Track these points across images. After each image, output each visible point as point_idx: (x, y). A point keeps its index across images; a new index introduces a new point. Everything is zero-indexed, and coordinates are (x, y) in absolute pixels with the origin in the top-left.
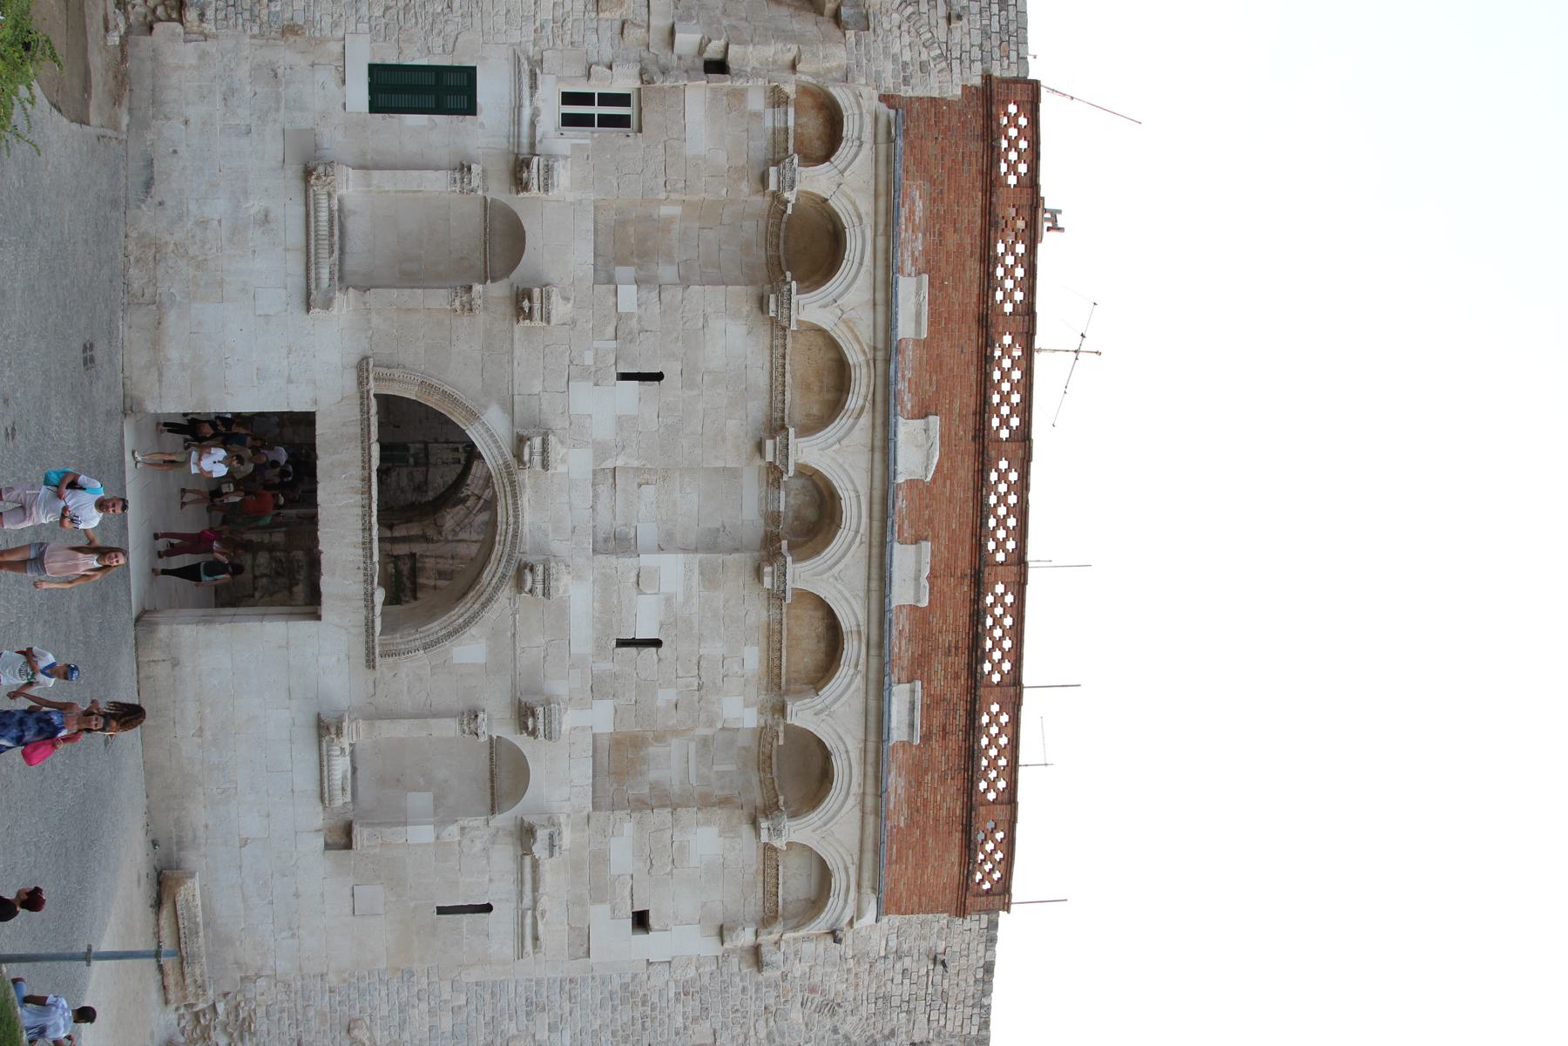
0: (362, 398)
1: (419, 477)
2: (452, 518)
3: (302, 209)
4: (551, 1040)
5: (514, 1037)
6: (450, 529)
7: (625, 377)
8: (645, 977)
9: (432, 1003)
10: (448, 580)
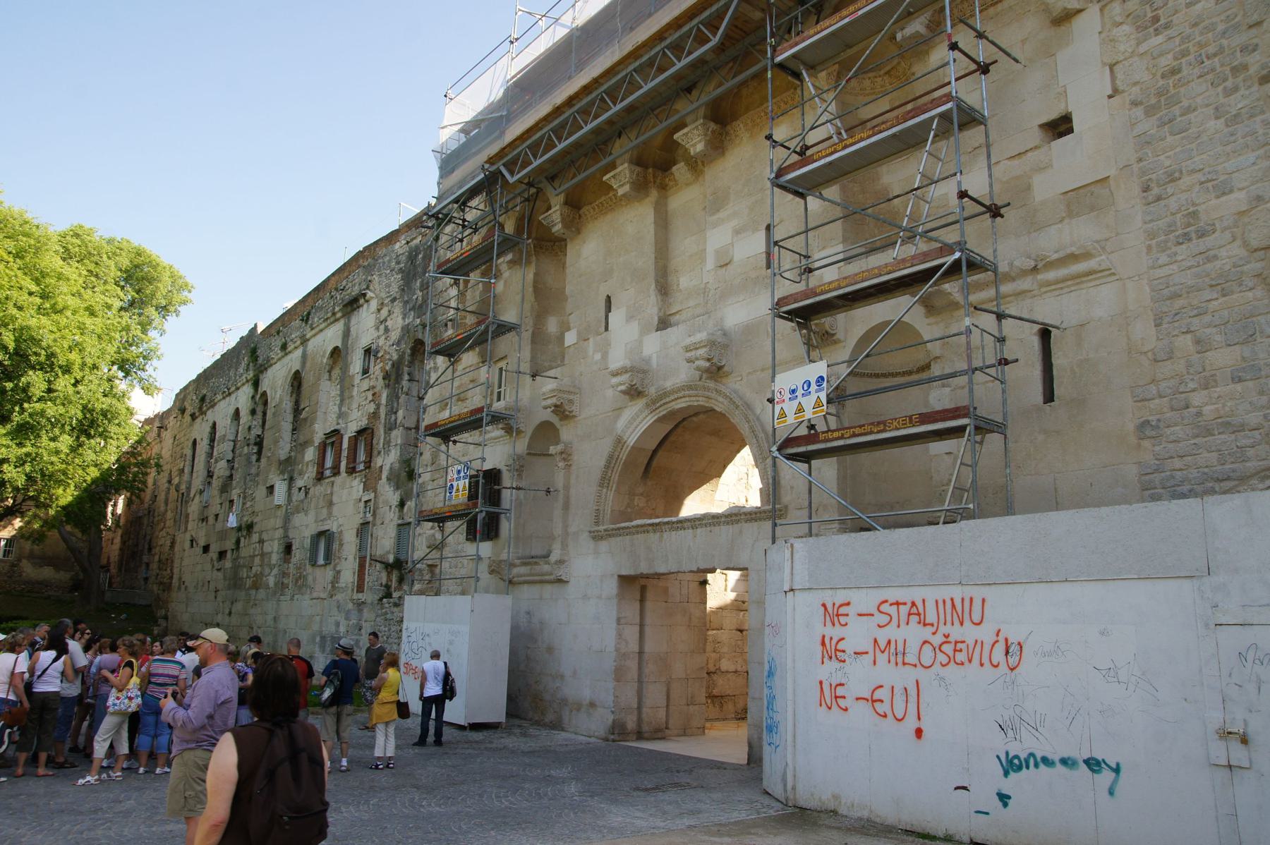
0: (610, 536)
3: (525, 587)
4: (1246, 184)
5: (1245, 244)
7: (607, 329)
8: (1136, 89)
9: (1191, 385)
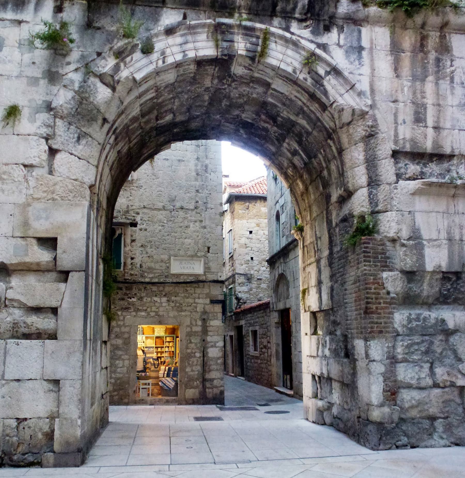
1: (241, 279)
2: (341, 95)
6: (358, 100)
10: (425, 109)
